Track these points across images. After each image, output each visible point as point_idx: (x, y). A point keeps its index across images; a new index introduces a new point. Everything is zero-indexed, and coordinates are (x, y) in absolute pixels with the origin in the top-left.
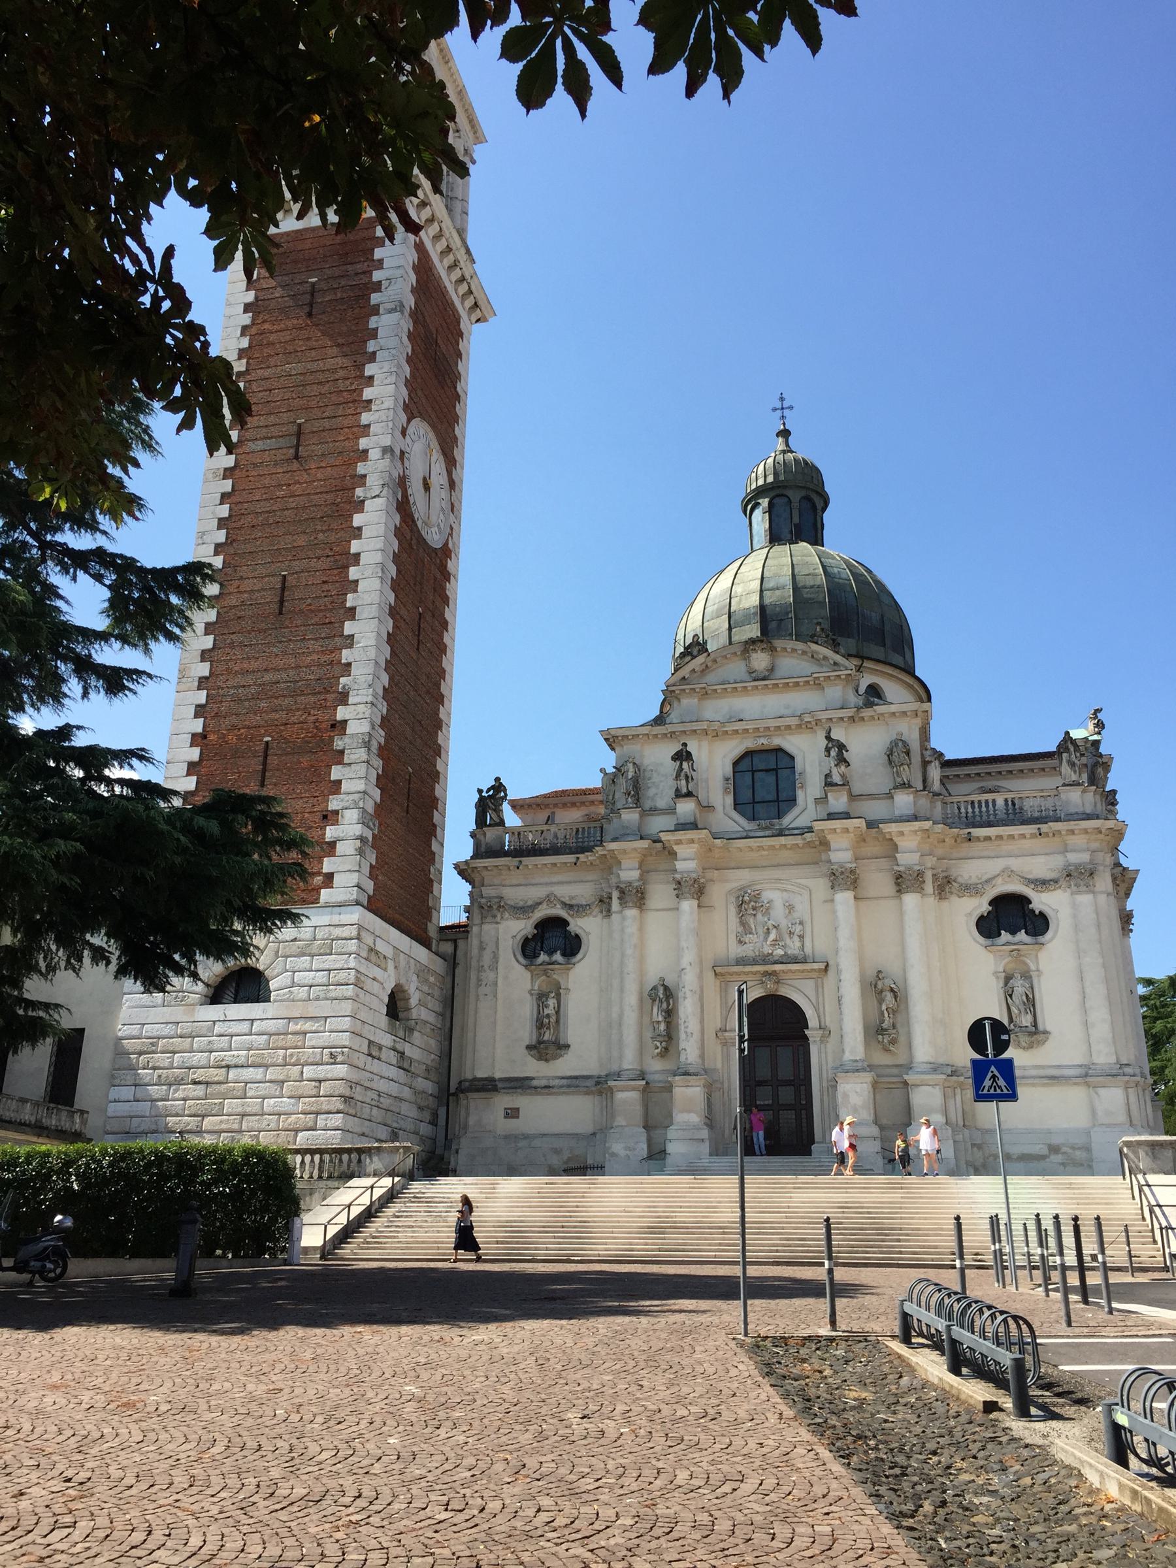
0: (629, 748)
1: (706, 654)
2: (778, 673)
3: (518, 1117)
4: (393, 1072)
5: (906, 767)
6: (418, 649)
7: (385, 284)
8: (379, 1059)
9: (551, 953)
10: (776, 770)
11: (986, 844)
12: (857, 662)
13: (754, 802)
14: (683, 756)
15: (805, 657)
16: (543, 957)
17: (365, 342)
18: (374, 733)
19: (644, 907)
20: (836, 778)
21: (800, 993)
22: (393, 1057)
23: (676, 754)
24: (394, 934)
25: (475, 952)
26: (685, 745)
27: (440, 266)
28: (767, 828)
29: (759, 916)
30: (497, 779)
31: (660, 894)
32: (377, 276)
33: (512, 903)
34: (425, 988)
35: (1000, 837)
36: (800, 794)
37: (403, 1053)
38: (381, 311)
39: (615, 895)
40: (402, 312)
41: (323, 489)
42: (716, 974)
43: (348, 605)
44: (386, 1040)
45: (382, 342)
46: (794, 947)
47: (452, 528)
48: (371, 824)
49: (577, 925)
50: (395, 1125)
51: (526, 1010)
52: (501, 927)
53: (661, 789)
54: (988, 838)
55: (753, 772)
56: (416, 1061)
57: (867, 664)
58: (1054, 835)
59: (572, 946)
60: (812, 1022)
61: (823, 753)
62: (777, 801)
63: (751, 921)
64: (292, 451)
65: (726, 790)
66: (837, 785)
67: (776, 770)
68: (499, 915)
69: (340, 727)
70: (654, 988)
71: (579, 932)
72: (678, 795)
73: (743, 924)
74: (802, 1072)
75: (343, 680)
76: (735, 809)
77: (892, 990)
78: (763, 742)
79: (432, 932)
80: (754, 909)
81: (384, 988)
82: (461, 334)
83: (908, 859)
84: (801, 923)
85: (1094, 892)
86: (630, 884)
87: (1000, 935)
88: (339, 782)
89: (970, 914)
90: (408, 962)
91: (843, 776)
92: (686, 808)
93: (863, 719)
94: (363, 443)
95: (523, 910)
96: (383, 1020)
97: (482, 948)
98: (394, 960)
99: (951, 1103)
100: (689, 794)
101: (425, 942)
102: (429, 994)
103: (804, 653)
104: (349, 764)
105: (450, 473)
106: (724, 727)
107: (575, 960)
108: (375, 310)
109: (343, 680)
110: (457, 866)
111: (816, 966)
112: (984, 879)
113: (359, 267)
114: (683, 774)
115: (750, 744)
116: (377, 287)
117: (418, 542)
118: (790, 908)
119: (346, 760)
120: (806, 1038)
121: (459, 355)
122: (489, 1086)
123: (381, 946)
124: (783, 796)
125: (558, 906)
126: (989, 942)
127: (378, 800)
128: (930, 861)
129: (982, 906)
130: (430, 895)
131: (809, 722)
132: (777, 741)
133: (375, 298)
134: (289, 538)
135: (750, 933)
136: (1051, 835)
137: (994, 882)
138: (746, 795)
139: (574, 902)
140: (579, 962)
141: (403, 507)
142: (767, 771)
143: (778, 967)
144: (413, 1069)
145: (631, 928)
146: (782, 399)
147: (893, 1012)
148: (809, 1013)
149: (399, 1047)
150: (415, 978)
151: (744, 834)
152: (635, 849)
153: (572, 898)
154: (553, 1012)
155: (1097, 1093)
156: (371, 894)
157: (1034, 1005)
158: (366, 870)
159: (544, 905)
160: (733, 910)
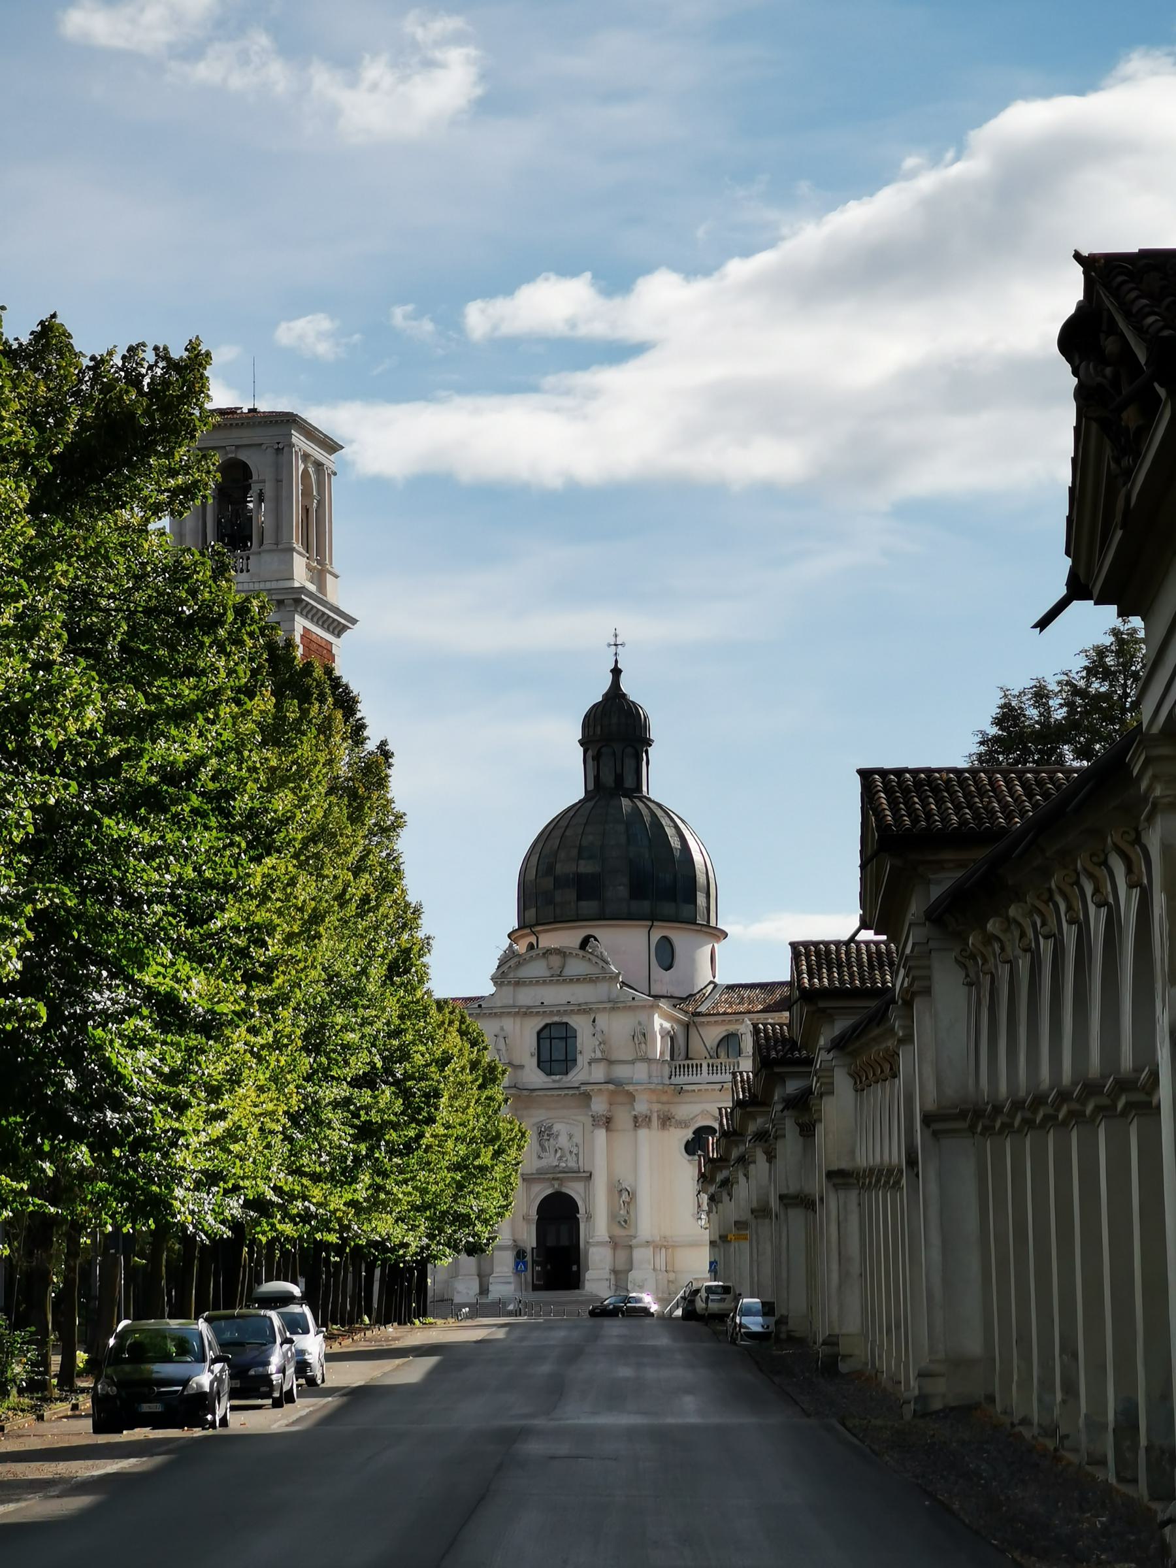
10: (566, 1038)
12: (649, 923)
21: (574, 1190)
29: (551, 1140)
36: (579, 1058)
46: (572, 1164)
55: (551, 1039)
60: (582, 1210)
63: (546, 1144)
65: (532, 1055)
67: (566, 1038)
78: (556, 1019)
99: (657, 1258)
115: (548, 1021)
118: (571, 1136)
128: (656, 1107)
129: (689, 1134)
132: (565, 1020)
138: (545, 1056)
147: (627, 1204)
148: (580, 1204)
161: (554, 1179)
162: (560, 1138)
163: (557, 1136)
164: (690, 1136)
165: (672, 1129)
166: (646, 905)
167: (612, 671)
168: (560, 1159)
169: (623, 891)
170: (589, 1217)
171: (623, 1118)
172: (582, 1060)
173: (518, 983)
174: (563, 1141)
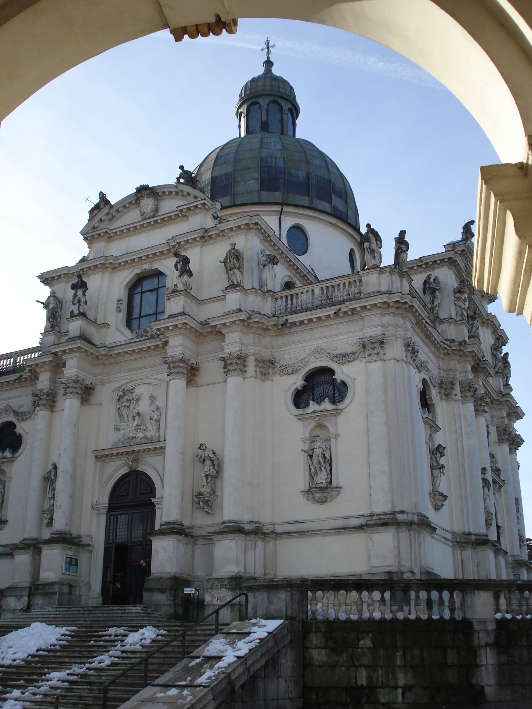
1: (108, 206)
2: (161, 212)
5: (236, 271)
10: (157, 289)
11: (303, 327)
12: (278, 208)
15: (172, 196)
19: (55, 409)
35: (310, 320)
42: (97, 457)
54: (302, 322)
57: (286, 209)
58: (353, 313)
63: (124, 411)
65: (119, 311)
67: (157, 289)
73: (120, 415)
78: (146, 267)
80: (128, 401)
85: (383, 360)
86: (41, 390)
89: (288, 391)
93: (210, 237)
106: (118, 260)
114: (76, 300)
115: (138, 271)
118: (152, 398)
120: (153, 505)
124: (159, 311)
125: (12, 414)
126: (300, 412)
131: (174, 246)
132: (156, 266)
135: (125, 422)
136: (350, 313)
139: (21, 410)
142: (151, 291)
151: (127, 342)
152: (44, 363)
153: (20, 407)
155: (371, 539)
157: (330, 464)
159: (4, 415)
160: (114, 406)
163: (138, 400)
165: (277, 378)
166: (278, 196)
167: (265, 63)
168: (138, 428)
169: (254, 185)
173: (110, 236)
174: (144, 406)
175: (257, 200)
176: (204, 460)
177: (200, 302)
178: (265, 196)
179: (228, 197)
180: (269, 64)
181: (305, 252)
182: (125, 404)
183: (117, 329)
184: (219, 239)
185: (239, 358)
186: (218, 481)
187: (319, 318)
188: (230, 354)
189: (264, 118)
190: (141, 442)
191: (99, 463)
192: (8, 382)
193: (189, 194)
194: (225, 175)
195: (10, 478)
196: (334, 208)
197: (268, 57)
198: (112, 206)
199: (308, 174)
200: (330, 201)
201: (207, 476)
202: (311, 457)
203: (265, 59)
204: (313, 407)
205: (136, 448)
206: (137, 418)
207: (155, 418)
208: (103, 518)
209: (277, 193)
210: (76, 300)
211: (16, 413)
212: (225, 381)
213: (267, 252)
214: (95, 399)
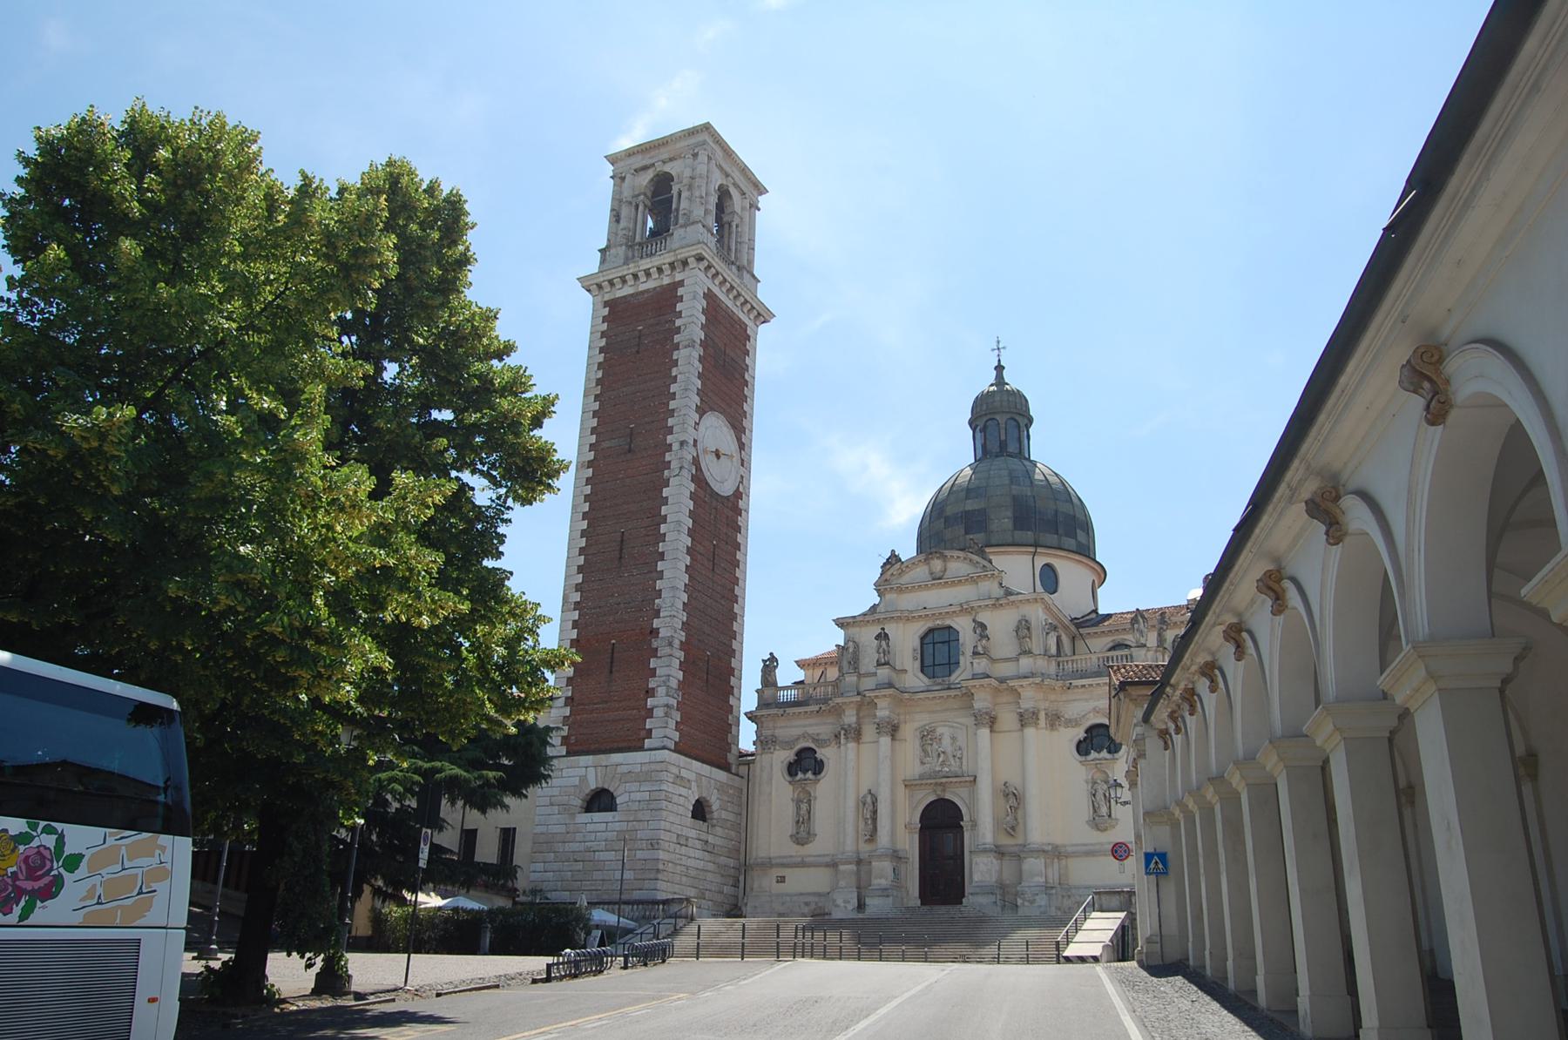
0: (853, 631)
2: (948, 574)
3: (784, 882)
4: (699, 854)
5: (1028, 639)
6: (713, 570)
7: (683, 328)
8: (686, 846)
9: (805, 771)
11: (1083, 689)
12: (1032, 549)
13: (934, 665)
14: (883, 636)
16: (800, 775)
17: (670, 370)
18: (676, 635)
20: (980, 649)
21: (957, 796)
22: (698, 844)
23: (877, 636)
24: (696, 764)
25: (758, 770)
26: (883, 629)
27: (727, 301)
28: (940, 684)
30: (771, 654)
31: (869, 731)
32: (678, 323)
33: (781, 739)
34: (726, 798)
35: (1091, 685)
36: (961, 658)
37: (707, 842)
38: (680, 347)
39: (843, 732)
40: (694, 347)
41: (645, 472)
42: (906, 786)
43: (660, 550)
44: (693, 834)
45: (681, 368)
46: (954, 766)
47: (742, 477)
48: (676, 695)
49: (821, 753)
50: (701, 887)
51: (790, 810)
52: (774, 756)
53: (868, 661)
56: (717, 846)
59: (818, 767)
61: (973, 633)
62: (949, 664)
63: (929, 748)
64: (627, 447)
65: (915, 659)
66: (980, 654)
68: (772, 748)
69: (654, 632)
70: (864, 797)
71: (823, 758)
72: (879, 664)
74: (959, 853)
75: (657, 601)
76: (922, 671)
77: (1014, 793)
78: (938, 622)
79: (731, 758)
80: (931, 739)
81: (689, 800)
82: (748, 338)
83: (1026, 704)
84: (960, 749)
86: (850, 726)
87: (1090, 753)
88: (655, 669)
90: (709, 782)
91: (984, 648)
92: (884, 673)
94: (669, 439)
95: (787, 744)
96: (689, 821)
97: (762, 770)
98: (696, 781)
100: (887, 663)
101: (725, 767)
102: (729, 802)
103: (965, 559)
104: (661, 657)
105: (739, 439)
107: (819, 777)
108: (677, 347)
109: (657, 601)
110: (746, 714)
111: (968, 779)
112: (1083, 713)
113: (668, 317)
115: (930, 624)
116: (678, 330)
117: (711, 496)
118: (954, 739)
119: (659, 655)
120: (962, 827)
121: (747, 353)
122: (768, 864)
123: (684, 773)
126: (1083, 758)
127: (681, 679)
129: (1080, 733)
130: (729, 735)
132: (948, 622)
133: (677, 338)
134: (625, 506)
137: (1088, 716)
138: (929, 661)
139: (821, 737)
140: (823, 778)
141: (699, 479)
143: (944, 780)
144: (715, 852)
145: (851, 755)
146: (998, 342)
147: (1014, 809)
148: (964, 810)
149: (704, 836)
150: (716, 791)
151: (925, 689)
152: (852, 702)
153: (818, 734)
154: (806, 813)
156: (677, 740)
158: (672, 724)
159: (801, 740)
160: (918, 742)
161: (936, 784)
162: (942, 741)
164: (1081, 735)
166: (1029, 536)
167: (996, 368)
169: (1007, 523)
170: (974, 824)
171: (1008, 719)
172: (965, 660)
175: (1010, 540)
176: (1008, 795)
177: (993, 661)
178: (1020, 535)
179: (983, 534)
180: (999, 368)
181: (1055, 592)
182: (930, 742)
183: (914, 675)
184: (1008, 607)
185: (1034, 713)
186: (1020, 812)
187: (1098, 684)
188: (1026, 710)
189: (1003, 438)
190: (947, 775)
191: (907, 791)
192: (806, 712)
193: (977, 562)
194: (978, 510)
195: (815, 798)
196: (1079, 544)
197: (999, 361)
198: (903, 563)
199: (1056, 511)
200: (1075, 537)
201: (1011, 807)
202: (1094, 795)
203: (996, 364)
204: (1093, 755)
205: (944, 780)
206: (942, 755)
207: (959, 755)
208: (917, 837)
209: (1029, 533)
210: (881, 650)
211: (815, 740)
212: (1022, 730)
213: (1050, 621)
214: (900, 735)
